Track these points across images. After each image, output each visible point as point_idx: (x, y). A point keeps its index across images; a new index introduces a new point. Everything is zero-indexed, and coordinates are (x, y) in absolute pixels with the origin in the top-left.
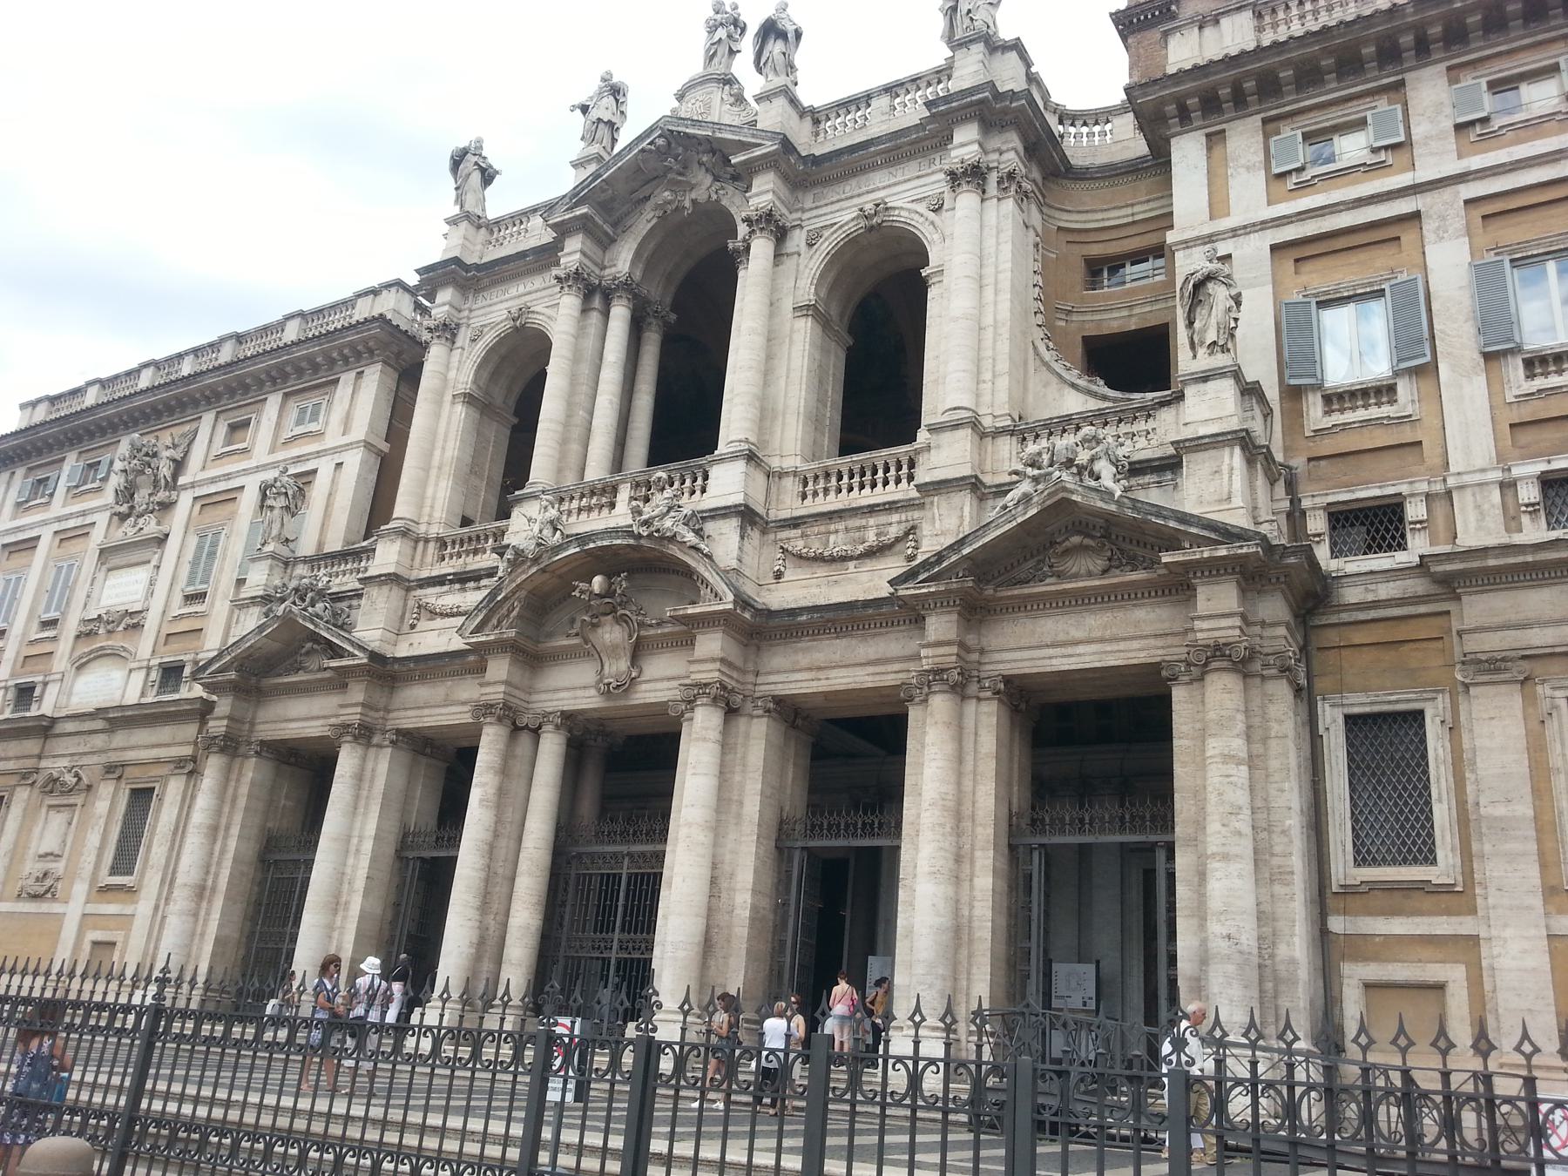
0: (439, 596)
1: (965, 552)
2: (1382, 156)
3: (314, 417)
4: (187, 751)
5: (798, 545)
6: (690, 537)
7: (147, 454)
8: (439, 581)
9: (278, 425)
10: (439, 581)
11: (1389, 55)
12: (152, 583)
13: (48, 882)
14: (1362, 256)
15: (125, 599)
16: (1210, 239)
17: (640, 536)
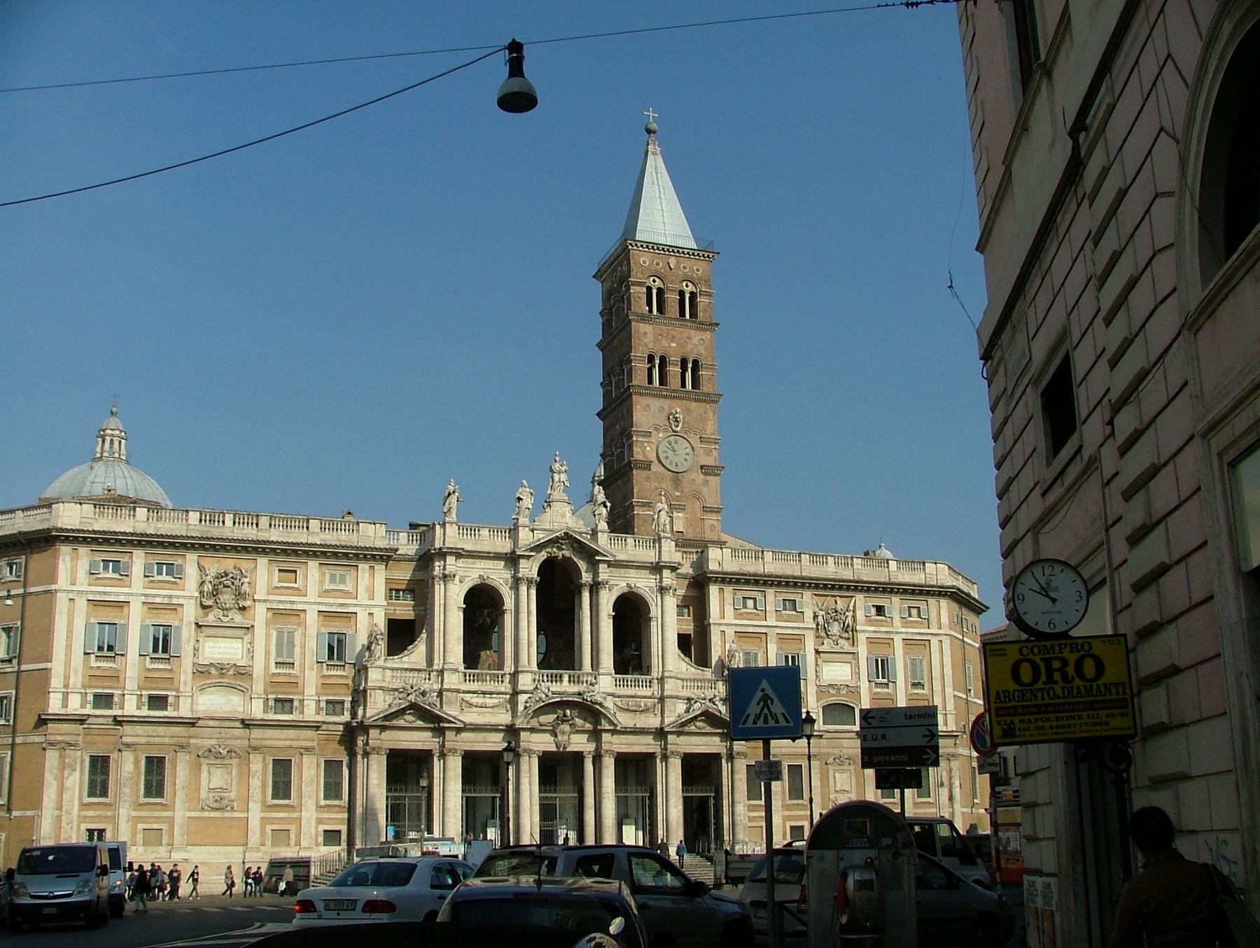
0: (472, 698)
1: (683, 720)
2: (760, 612)
3: (343, 581)
4: (310, 744)
5: (619, 704)
6: (606, 705)
7: (232, 578)
8: (474, 692)
9: (322, 583)
10: (474, 692)
11: (765, 583)
12: (251, 652)
13: (225, 802)
14: (752, 640)
15: (229, 657)
16: (720, 624)
17: (587, 701)
